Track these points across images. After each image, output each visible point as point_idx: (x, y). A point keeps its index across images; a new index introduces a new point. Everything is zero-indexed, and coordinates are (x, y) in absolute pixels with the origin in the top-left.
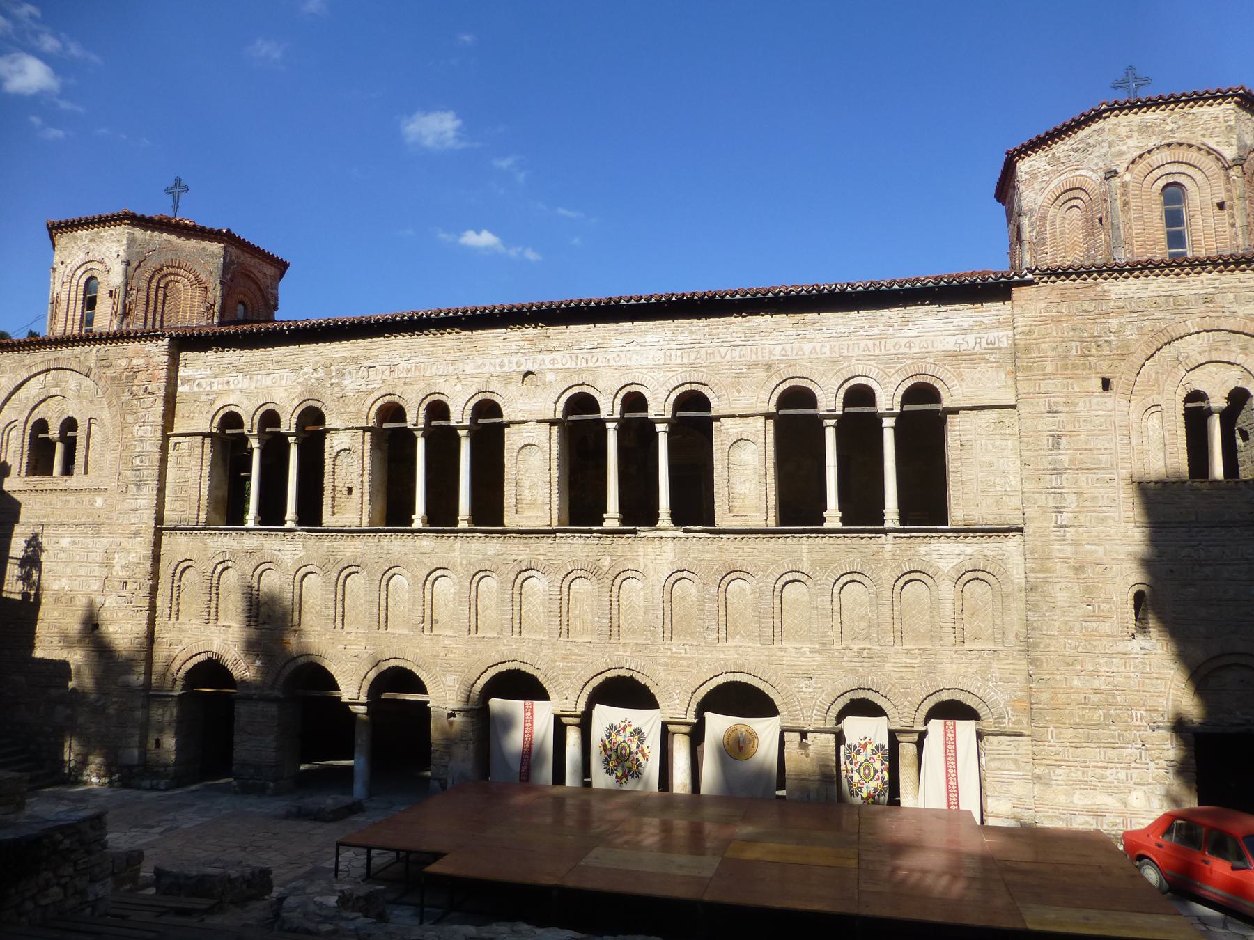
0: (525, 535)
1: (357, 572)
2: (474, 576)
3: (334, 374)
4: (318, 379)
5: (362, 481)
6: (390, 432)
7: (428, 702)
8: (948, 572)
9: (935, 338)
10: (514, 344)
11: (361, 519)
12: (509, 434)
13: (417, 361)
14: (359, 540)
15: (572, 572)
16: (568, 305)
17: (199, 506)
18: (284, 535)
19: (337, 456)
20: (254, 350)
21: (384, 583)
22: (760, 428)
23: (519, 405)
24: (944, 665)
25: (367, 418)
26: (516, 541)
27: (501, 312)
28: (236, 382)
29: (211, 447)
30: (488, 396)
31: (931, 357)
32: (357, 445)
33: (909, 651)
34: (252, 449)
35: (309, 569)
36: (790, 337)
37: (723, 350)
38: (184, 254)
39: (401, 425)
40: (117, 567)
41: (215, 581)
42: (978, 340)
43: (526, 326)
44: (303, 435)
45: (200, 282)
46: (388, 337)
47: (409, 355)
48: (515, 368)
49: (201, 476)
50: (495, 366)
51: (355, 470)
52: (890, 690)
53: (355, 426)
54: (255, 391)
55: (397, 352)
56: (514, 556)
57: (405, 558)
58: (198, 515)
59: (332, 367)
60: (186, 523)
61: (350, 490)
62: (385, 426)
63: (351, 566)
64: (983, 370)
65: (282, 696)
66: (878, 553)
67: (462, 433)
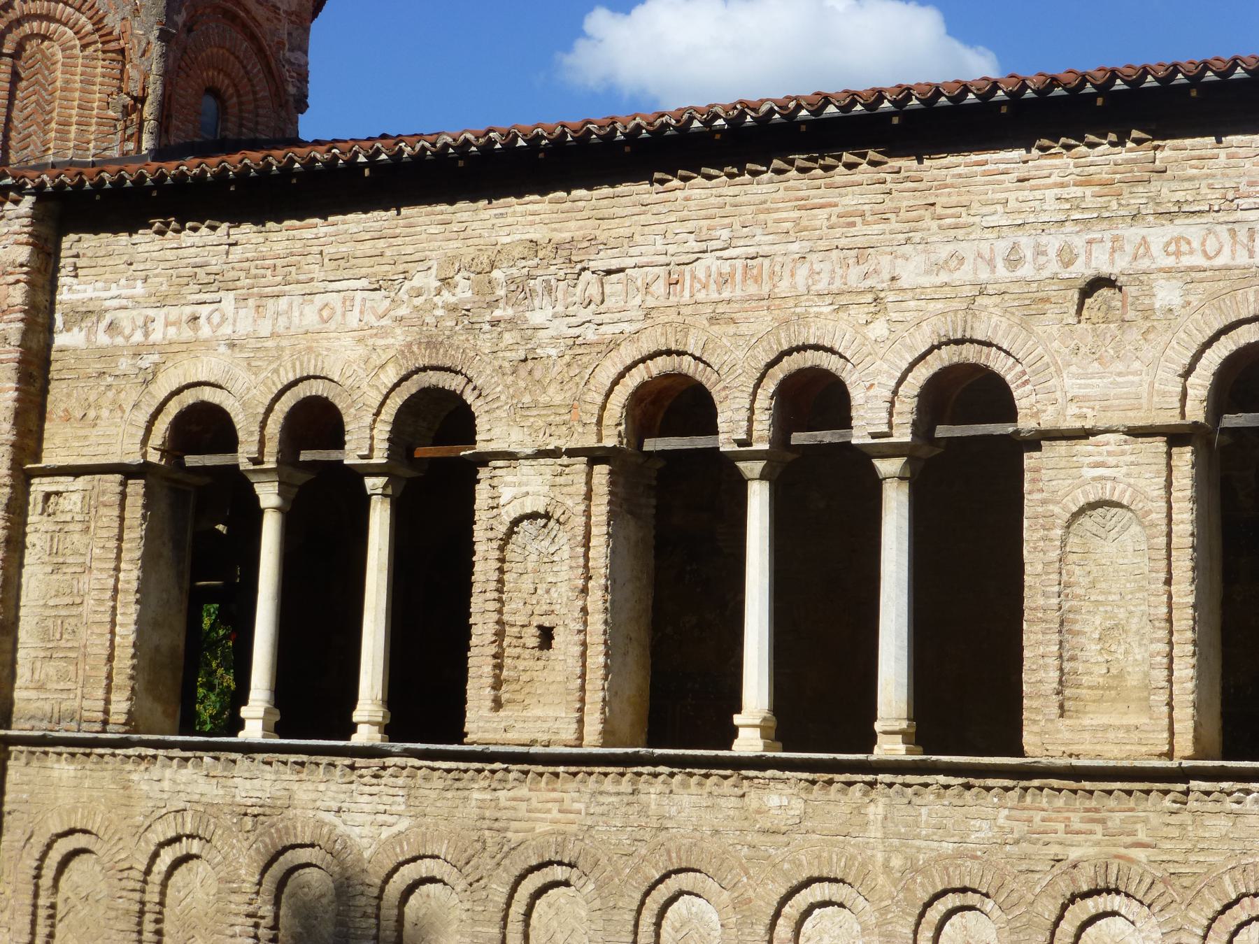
0: (1087, 785)
1: (566, 884)
2: (928, 905)
3: (501, 292)
4: (454, 309)
5: (584, 610)
6: (660, 464)
10: (1051, 194)
11: (581, 721)
12: (1037, 470)
13: (751, 251)
14: (573, 785)
15: (1237, 901)
16: (1224, 74)
17: (109, 677)
18: (352, 768)
19: (511, 532)
20: (271, 225)
21: (648, 919)
23: (1068, 382)
25: (599, 422)
26: (1060, 801)
27: (1015, 96)
28: (216, 318)
29: (145, 507)
30: (969, 354)
32: (569, 503)
34: (259, 513)
39: (701, 442)
41: (152, 896)
43: (1091, 138)
44: (407, 472)
45: (107, 37)
46: (662, 182)
47: (725, 234)
48: (1054, 267)
49: (116, 590)
50: (991, 263)
51: (564, 576)
53: (564, 444)
54: (270, 344)
55: (690, 226)
56: (1054, 850)
57: (711, 845)
58: (108, 701)
59: (497, 274)
60: (74, 725)
61: (546, 636)
62: (651, 445)
63: (550, 863)
67: (887, 467)
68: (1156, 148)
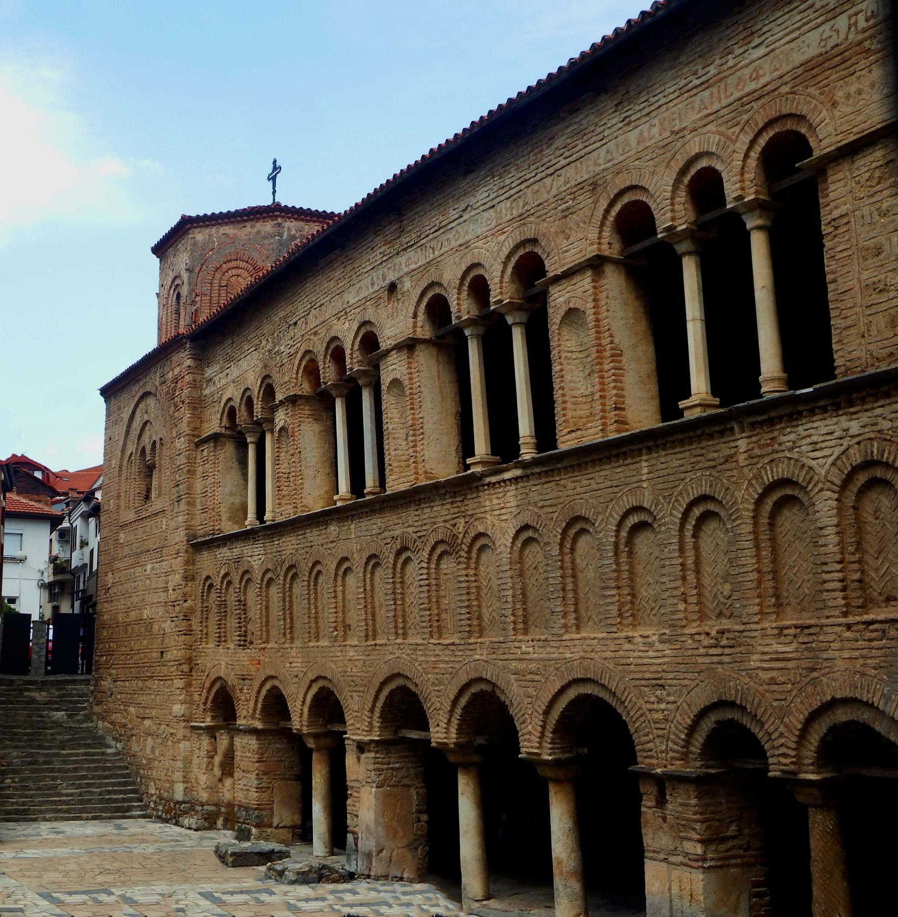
7: (346, 733)
8: (828, 472)
9: (792, 45)
22: (587, 287)
24: (830, 654)
31: (786, 84)
33: (782, 629)
35: (269, 575)
36: (615, 129)
37: (548, 181)
38: (241, 243)
40: (171, 591)
42: (853, 20)
52: (759, 704)
64: (864, 72)
65: (259, 727)
66: (731, 456)
68: (402, 221)
